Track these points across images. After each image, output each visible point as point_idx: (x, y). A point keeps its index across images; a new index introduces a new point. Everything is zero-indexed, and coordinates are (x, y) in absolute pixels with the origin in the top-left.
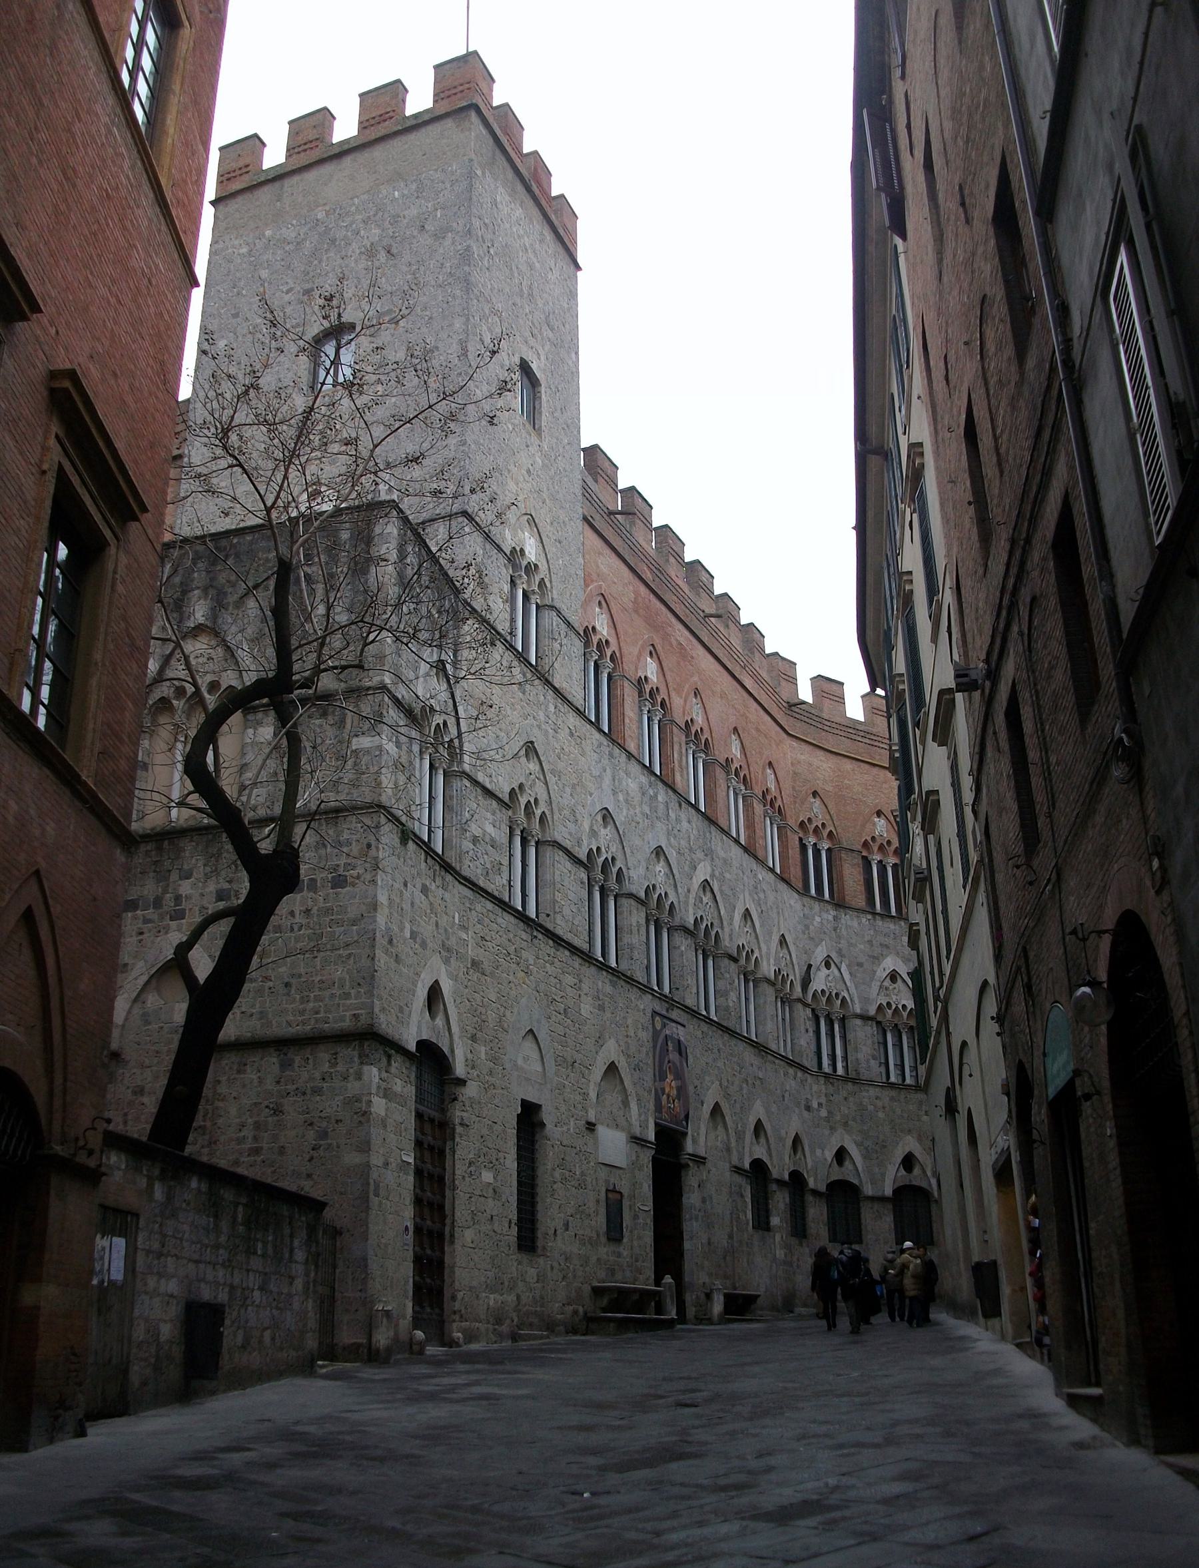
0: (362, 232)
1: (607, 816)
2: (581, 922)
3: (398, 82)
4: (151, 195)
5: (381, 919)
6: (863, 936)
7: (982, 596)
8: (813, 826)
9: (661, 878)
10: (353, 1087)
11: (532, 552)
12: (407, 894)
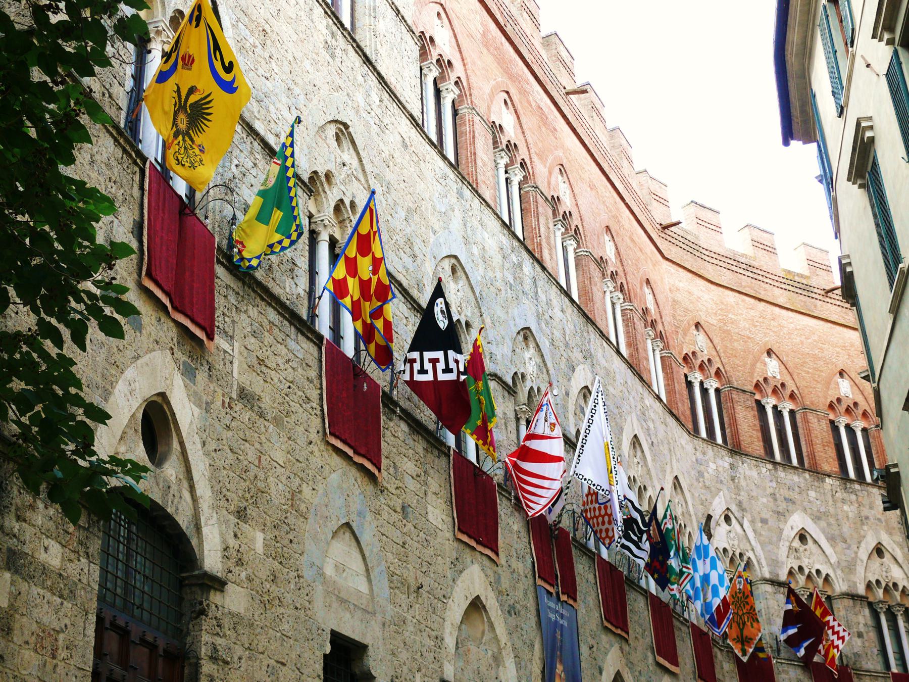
6: (765, 489)
8: (699, 362)
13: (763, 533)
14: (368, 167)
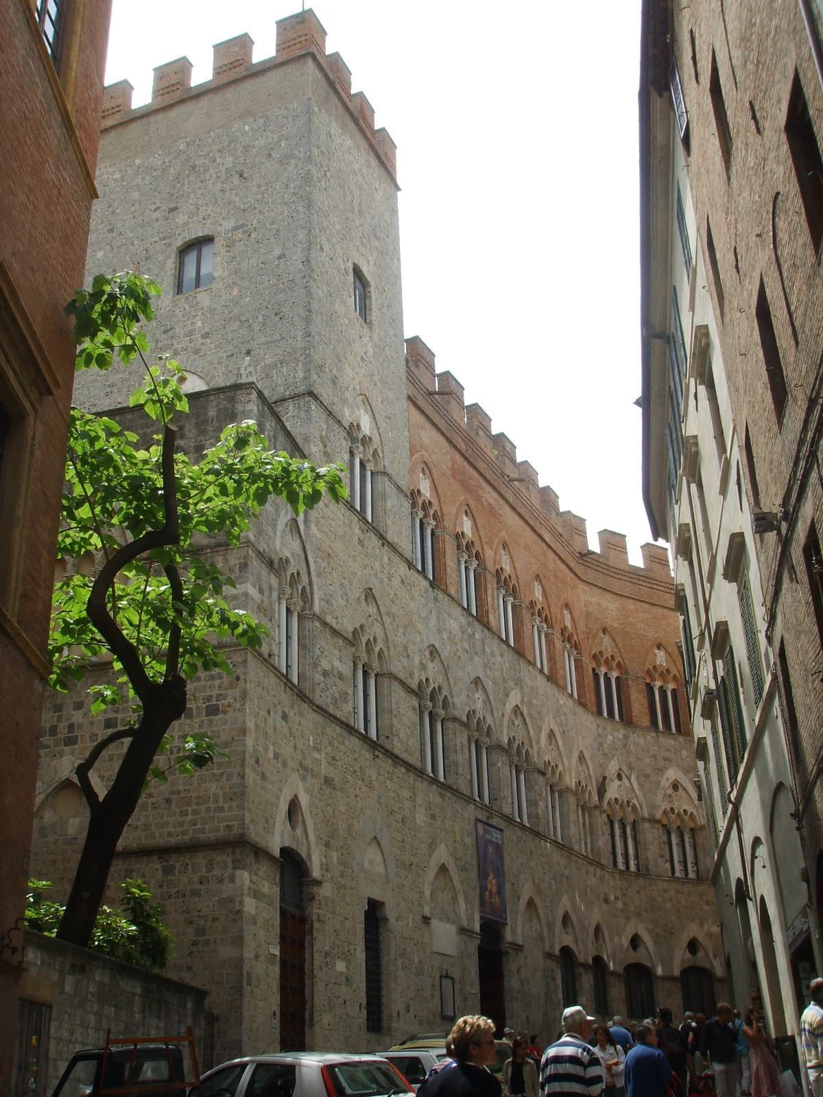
0: (218, 160)
1: (433, 652)
2: (414, 743)
3: (246, 36)
4: (59, 119)
5: (250, 742)
7: (777, 449)
9: (479, 705)
10: (227, 889)
11: (366, 427)
12: (270, 720)
13: (645, 785)
14: (383, 610)
